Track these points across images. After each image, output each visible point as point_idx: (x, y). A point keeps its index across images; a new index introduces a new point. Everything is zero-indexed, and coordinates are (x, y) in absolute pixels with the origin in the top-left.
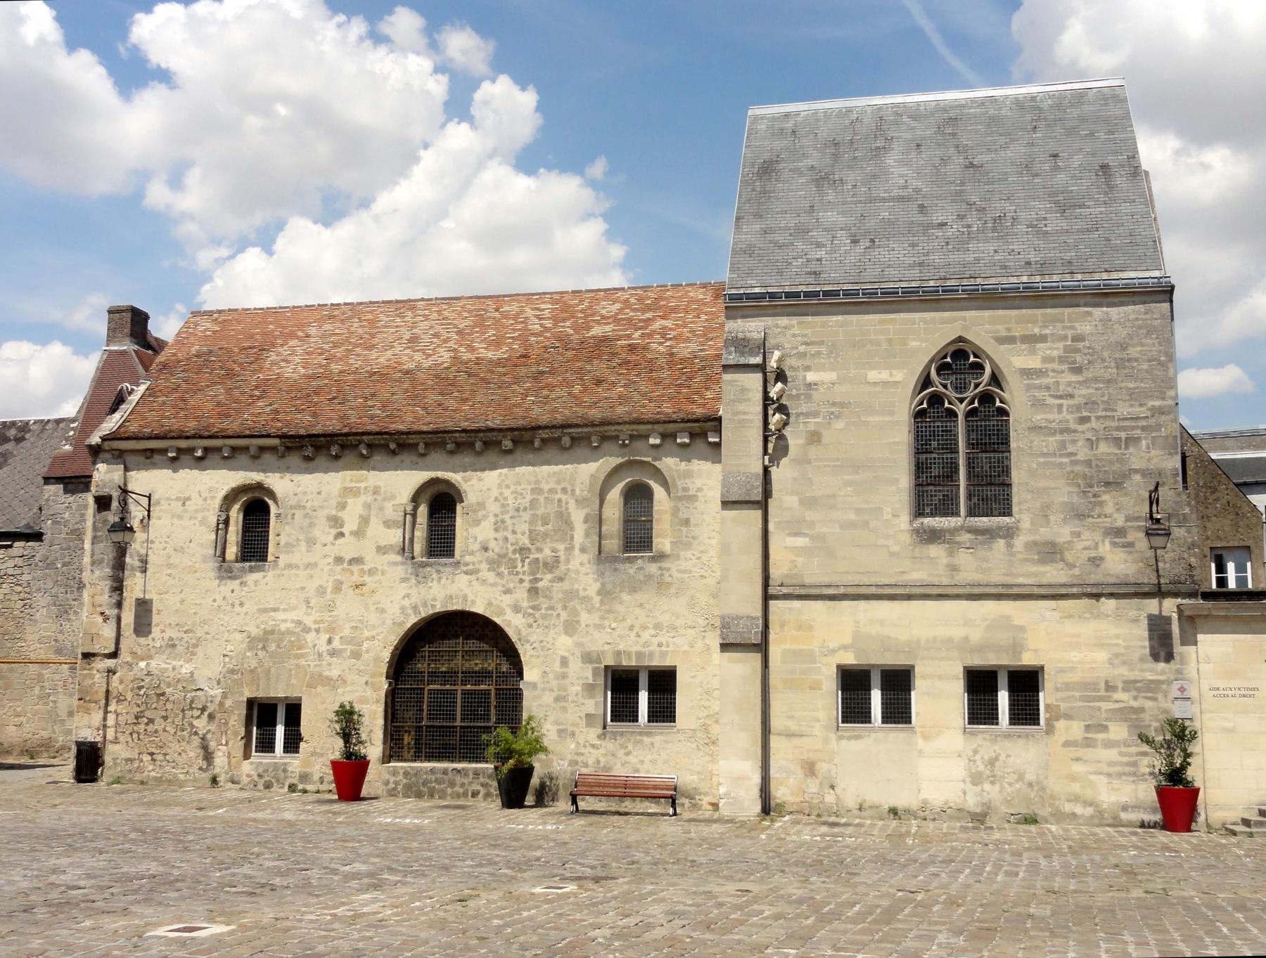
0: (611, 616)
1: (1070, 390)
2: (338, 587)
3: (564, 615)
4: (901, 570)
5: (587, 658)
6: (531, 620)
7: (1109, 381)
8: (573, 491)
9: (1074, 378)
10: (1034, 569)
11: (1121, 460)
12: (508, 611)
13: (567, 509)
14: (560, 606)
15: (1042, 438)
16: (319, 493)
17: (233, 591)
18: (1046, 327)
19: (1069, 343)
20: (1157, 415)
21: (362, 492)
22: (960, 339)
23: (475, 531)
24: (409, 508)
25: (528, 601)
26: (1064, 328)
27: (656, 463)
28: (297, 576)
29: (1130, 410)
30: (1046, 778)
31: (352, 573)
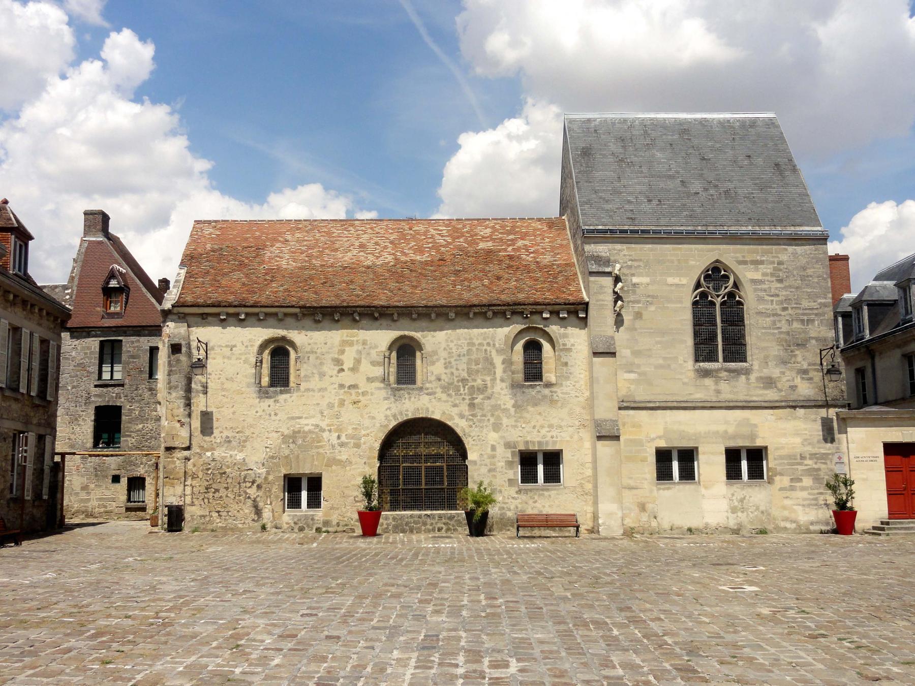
0: (522, 420)
1: (777, 291)
2: (342, 403)
3: (492, 420)
5: (508, 445)
6: (471, 423)
7: (797, 288)
8: (494, 345)
9: (779, 285)
11: (805, 332)
12: (456, 417)
14: (489, 414)
16: (326, 344)
17: (269, 406)
21: (355, 343)
23: (430, 368)
24: (387, 354)
25: (469, 410)
27: (546, 329)
28: (314, 396)
29: (809, 304)
31: (351, 394)
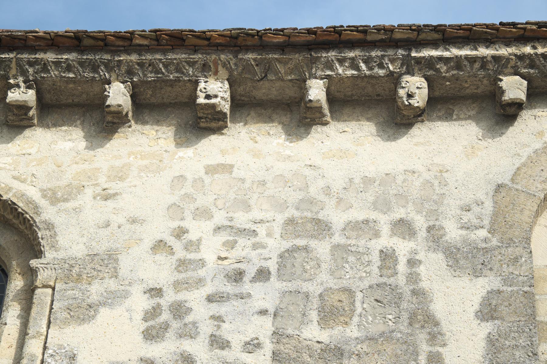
13: (413, 278)
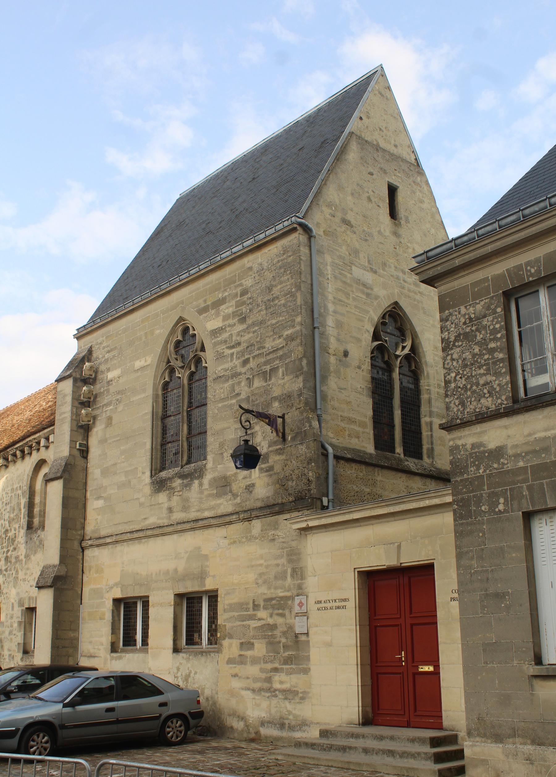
0: (28, 572)
1: (238, 338)
4: (144, 517)
7: (261, 323)
10: (213, 503)
11: (267, 391)
15: (221, 386)
18: (225, 290)
19: (239, 299)
20: (289, 342)
22: (181, 319)
26: (236, 287)
30: (217, 693)
